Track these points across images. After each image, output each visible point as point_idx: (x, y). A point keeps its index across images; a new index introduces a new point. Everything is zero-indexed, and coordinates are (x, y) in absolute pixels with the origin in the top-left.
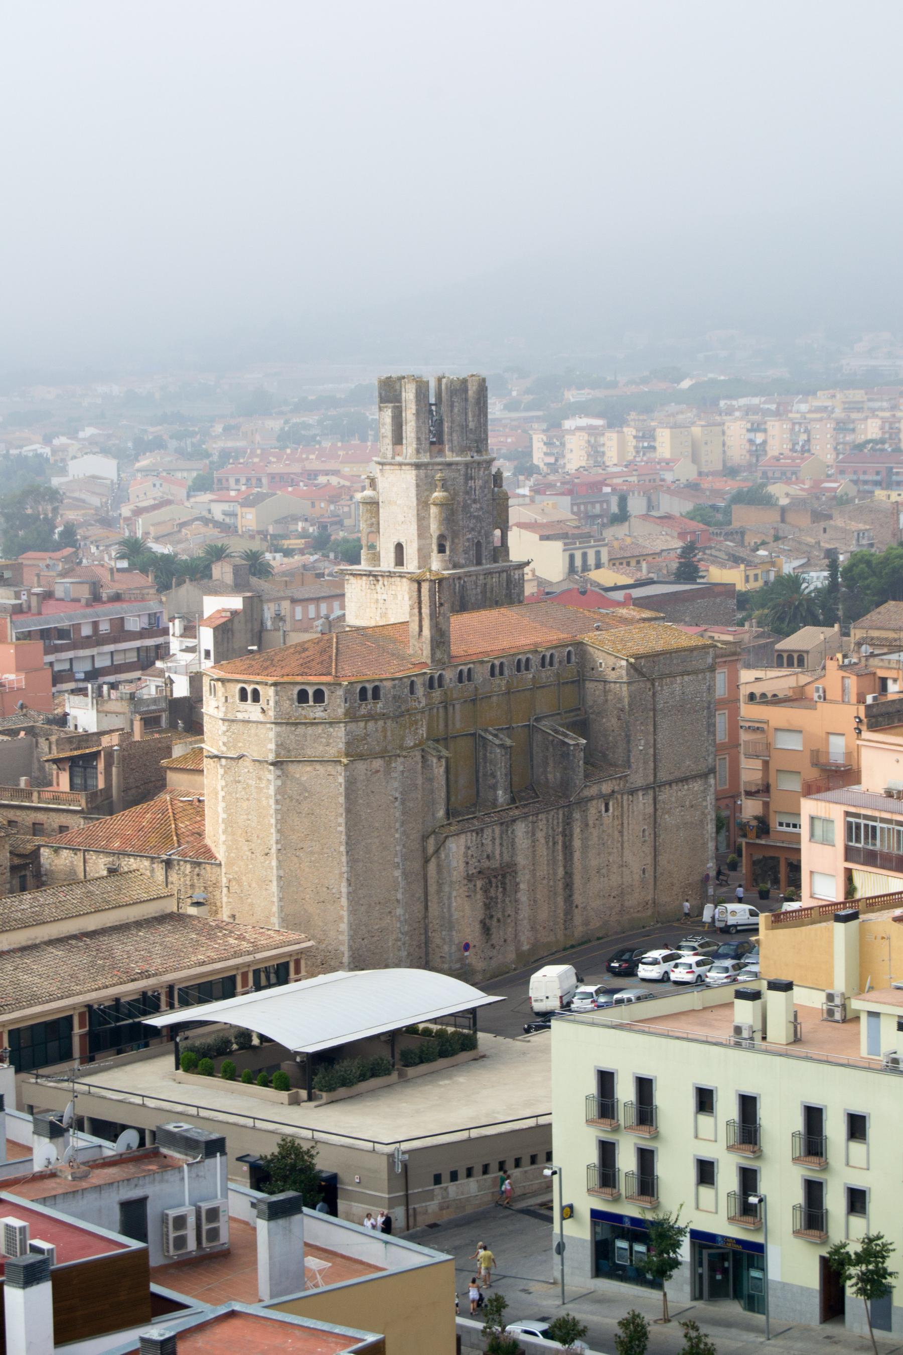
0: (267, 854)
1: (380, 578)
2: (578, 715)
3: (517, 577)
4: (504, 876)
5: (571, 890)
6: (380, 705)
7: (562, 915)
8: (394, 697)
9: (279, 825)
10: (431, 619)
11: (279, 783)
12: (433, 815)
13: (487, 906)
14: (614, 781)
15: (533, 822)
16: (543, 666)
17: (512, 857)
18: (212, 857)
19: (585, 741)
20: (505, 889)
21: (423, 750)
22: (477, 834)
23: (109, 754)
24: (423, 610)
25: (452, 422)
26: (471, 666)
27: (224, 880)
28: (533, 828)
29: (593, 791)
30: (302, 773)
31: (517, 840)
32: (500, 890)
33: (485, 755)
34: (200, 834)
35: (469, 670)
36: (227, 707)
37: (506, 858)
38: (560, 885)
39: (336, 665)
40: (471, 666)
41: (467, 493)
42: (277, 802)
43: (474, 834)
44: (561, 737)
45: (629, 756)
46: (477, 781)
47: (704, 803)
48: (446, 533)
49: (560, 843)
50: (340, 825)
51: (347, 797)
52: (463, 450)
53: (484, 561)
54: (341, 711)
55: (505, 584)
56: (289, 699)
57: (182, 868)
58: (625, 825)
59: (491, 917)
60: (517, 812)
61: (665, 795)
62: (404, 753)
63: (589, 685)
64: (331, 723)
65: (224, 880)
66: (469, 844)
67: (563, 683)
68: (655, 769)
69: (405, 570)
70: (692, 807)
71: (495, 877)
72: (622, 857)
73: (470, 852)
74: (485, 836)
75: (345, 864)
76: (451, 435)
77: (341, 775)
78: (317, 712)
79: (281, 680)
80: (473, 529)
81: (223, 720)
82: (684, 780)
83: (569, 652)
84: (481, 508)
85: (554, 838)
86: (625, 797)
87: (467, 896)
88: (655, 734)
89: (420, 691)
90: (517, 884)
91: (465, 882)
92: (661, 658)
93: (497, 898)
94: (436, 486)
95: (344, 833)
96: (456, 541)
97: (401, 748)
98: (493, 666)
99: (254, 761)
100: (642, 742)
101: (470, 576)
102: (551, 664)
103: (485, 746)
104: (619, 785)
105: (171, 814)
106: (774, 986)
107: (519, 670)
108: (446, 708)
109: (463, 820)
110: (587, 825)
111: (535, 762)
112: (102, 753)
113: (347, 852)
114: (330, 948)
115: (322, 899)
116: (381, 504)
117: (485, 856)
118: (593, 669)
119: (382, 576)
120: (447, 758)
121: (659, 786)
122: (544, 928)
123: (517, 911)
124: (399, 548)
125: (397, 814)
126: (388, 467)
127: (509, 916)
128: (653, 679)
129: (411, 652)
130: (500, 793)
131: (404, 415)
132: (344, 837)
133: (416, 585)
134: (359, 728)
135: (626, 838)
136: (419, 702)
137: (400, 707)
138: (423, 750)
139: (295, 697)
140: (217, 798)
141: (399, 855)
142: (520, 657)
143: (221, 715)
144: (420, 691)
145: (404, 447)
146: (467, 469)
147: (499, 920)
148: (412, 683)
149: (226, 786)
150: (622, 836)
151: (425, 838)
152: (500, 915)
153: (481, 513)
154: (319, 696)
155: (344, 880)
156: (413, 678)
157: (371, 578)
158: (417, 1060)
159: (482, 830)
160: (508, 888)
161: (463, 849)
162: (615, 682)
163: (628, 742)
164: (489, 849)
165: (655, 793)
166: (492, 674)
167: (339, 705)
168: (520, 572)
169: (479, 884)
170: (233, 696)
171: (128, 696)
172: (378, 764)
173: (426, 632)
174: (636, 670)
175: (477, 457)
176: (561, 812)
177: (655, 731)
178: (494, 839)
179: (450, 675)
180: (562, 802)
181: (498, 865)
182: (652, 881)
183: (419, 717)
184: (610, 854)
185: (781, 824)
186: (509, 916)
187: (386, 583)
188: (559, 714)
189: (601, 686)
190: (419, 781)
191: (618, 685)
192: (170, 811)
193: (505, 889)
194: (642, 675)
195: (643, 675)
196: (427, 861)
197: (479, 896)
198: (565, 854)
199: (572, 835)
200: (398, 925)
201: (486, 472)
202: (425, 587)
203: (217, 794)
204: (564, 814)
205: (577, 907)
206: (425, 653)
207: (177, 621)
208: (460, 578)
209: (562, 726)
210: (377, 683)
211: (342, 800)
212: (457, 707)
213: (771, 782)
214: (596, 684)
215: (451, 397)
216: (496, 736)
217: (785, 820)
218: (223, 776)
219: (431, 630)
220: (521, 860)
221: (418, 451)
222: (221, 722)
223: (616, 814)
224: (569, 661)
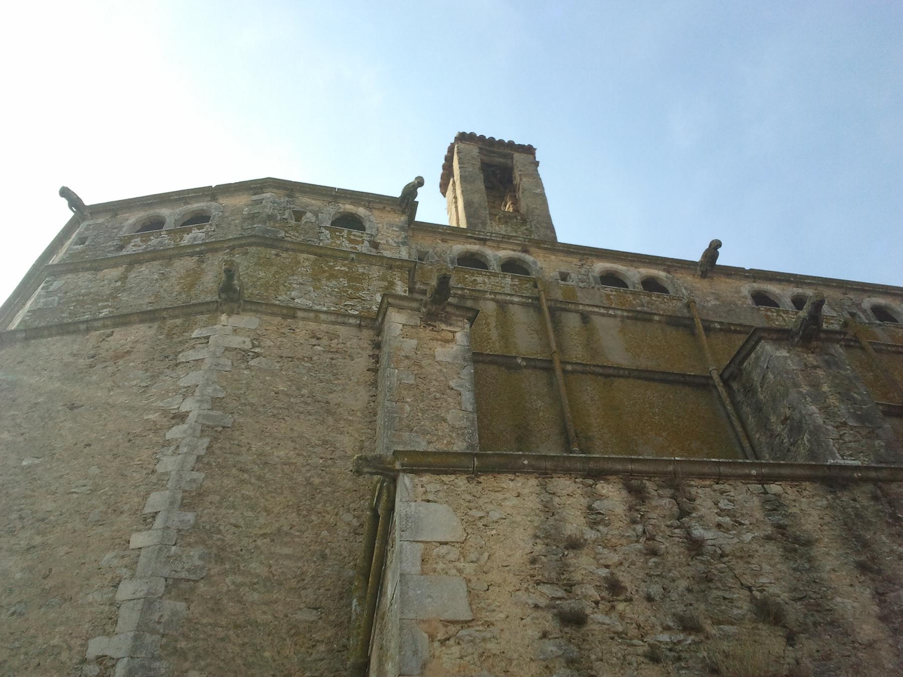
22: (638, 493)
66: (574, 523)
73: (583, 564)
161: (517, 545)
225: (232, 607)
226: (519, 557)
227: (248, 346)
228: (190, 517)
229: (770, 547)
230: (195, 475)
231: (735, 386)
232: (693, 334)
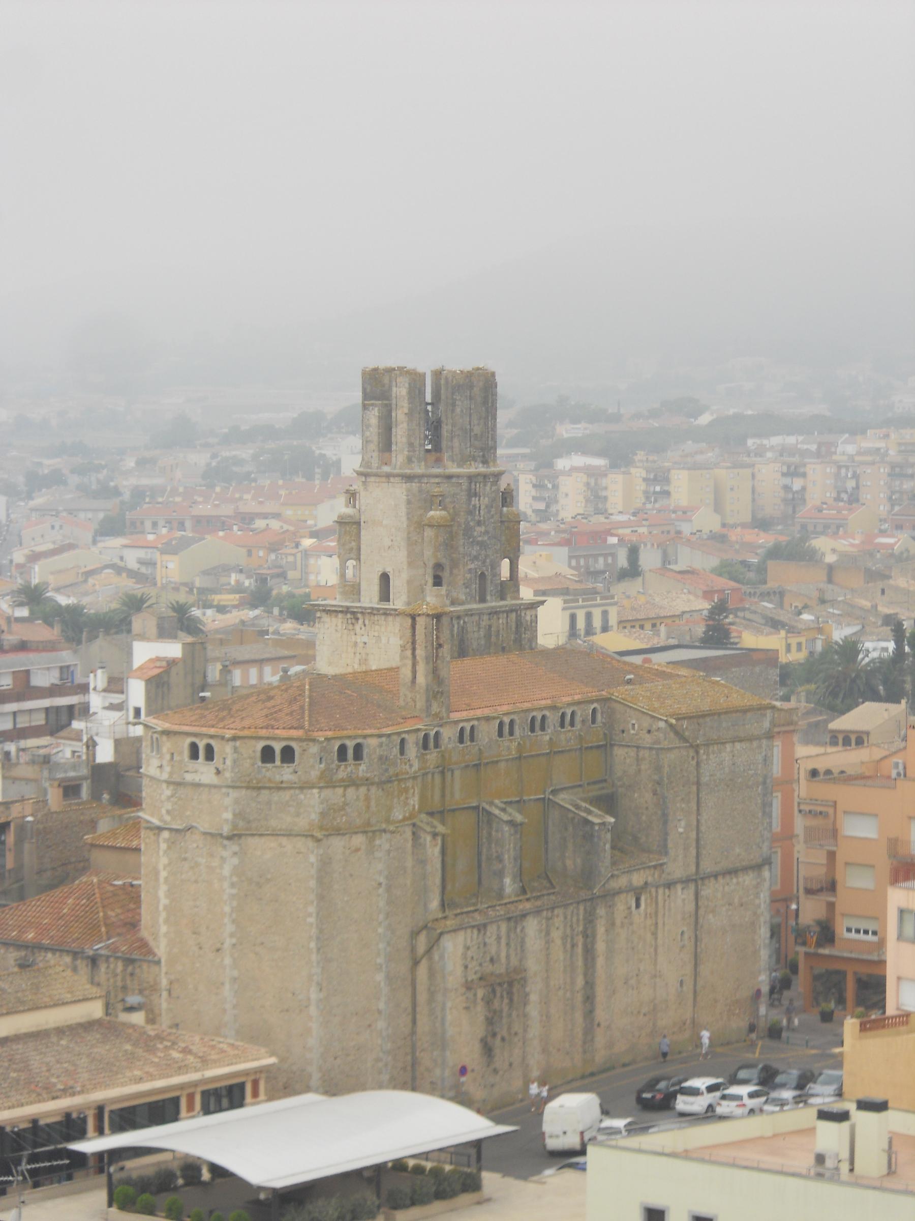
0: (218, 950)
1: (359, 615)
2: (603, 788)
3: (528, 618)
4: (511, 984)
6: (362, 769)
8: (380, 758)
9: (234, 916)
10: (427, 663)
11: (235, 861)
12: (425, 905)
13: (490, 1022)
14: (647, 872)
15: (548, 919)
16: (562, 725)
17: (521, 960)
18: (150, 952)
19: (612, 820)
20: (511, 1000)
21: (414, 825)
22: (479, 930)
23: (22, 827)
24: (418, 652)
25: (453, 425)
26: (476, 723)
27: (164, 982)
29: (622, 881)
30: (262, 850)
31: (527, 940)
32: (506, 1001)
33: (490, 834)
34: (133, 925)
35: (472, 728)
36: (172, 766)
37: (514, 961)
38: (579, 998)
39: (310, 716)
40: (476, 723)
41: (470, 513)
42: (233, 885)
43: (475, 931)
44: (583, 814)
45: (666, 840)
46: (479, 866)
47: (757, 901)
48: (443, 561)
50: (310, 915)
51: (320, 880)
52: (463, 460)
53: (488, 598)
54: (314, 774)
55: (514, 629)
56: (250, 758)
57: (112, 966)
59: (494, 1035)
60: (528, 906)
61: (709, 890)
62: (392, 828)
63: (619, 752)
64: (301, 788)
65: (164, 982)
67: (587, 748)
69: (392, 607)
71: (500, 984)
72: (655, 964)
73: (469, 953)
74: (488, 933)
75: (315, 964)
76: (452, 441)
77: (312, 852)
78: (286, 773)
79: (241, 734)
80: (476, 558)
81: (168, 783)
82: (732, 872)
83: (594, 710)
84: (486, 532)
85: (572, 938)
86: (661, 891)
87: (467, 1008)
88: (698, 813)
89: (412, 751)
90: (527, 995)
91: (464, 990)
92: (708, 719)
93: (501, 1011)
94: (432, 503)
95: (314, 926)
96: (455, 571)
97: (388, 821)
98: (501, 724)
99: (205, 834)
100: (683, 823)
101: (472, 615)
102: (572, 724)
103: (489, 823)
105: (98, 900)
106: (865, 1105)
107: (532, 730)
108: (442, 773)
109: (462, 913)
110: (613, 924)
112: (12, 825)
113: (318, 950)
116: (362, 523)
117: (488, 959)
118: (623, 732)
119: (362, 613)
120: (443, 836)
121: (702, 879)
122: (559, 1050)
123: (526, 1029)
124: (385, 578)
125: (382, 904)
126: (372, 479)
127: (516, 1034)
128: (698, 746)
129: (402, 703)
130: (507, 881)
131: (394, 414)
132: (314, 931)
133: (410, 621)
134: (335, 795)
135: (660, 942)
136: (411, 766)
137: (387, 770)
138: (414, 825)
139: (259, 754)
140: (157, 879)
142: (534, 713)
143: (165, 776)
144: (412, 751)
145: (394, 455)
146: (470, 483)
147: (503, 1039)
148: (403, 741)
149: (170, 864)
150: (656, 939)
151: (414, 934)
152: (504, 1033)
153: (486, 538)
154: (288, 755)
156: (403, 736)
157: (349, 616)
158: (408, 1202)
159: (485, 926)
160: (515, 998)
161: (460, 950)
162: (650, 749)
163: (665, 823)
164: (493, 950)
165: (697, 886)
166: (500, 734)
168: (533, 612)
169: (480, 993)
170: (181, 753)
171: (41, 759)
172: (359, 840)
173: (421, 679)
174: (677, 733)
175: (482, 469)
176: (582, 908)
177: (698, 809)
178: (499, 938)
179: (448, 734)
180: (583, 894)
181: (503, 970)
182: (691, 996)
183: (410, 784)
185: (849, 930)
187: (367, 622)
188: (580, 786)
189: (632, 753)
190: (409, 863)
191: (654, 752)
192: (97, 895)
193: (511, 1000)
194: (685, 740)
195: (685, 740)
196: (416, 963)
197: (480, 1008)
198: (586, 959)
199: (594, 937)
200: (379, 1042)
201: (494, 488)
202: (421, 622)
203: (157, 873)
204: (585, 909)
205: (599, 1025)
206: (419, 705)
207: (99, 672)
208: (459, 618)
209: (584, 800)
210: (359, 741)
211: (313, 883)
212: (457, 773)
213: (838, 877)
214: (626, 750)
215: (453, 394)
216: (504, 810)
217: (854, 924)
218: (165, 852)
219: (426, 676)
220: (533, 965)
221: (409, 460)
222: (164, 786)
223: (649, 911)
224: (594, 721)
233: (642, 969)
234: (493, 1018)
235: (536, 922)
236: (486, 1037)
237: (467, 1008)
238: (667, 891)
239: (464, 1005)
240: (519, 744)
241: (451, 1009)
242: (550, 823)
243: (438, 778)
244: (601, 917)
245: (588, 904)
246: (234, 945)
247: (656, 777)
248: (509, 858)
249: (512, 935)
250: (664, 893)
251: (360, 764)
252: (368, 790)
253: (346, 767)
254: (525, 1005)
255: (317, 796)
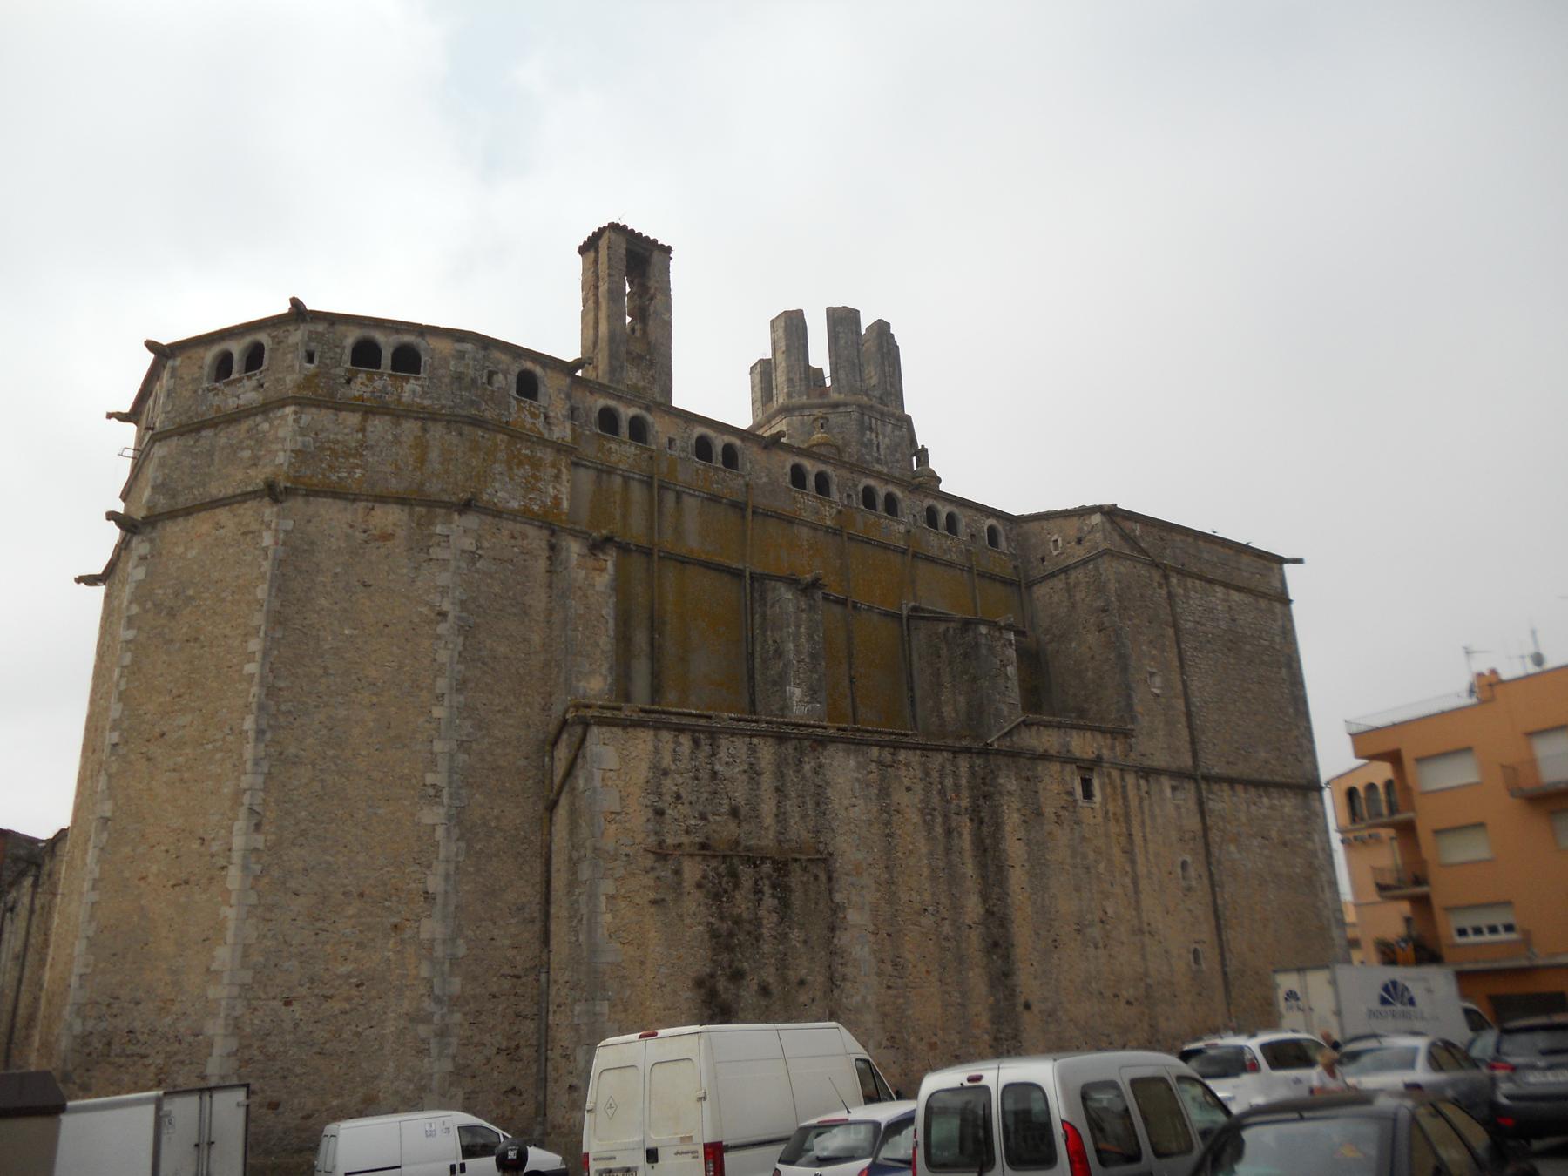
4: (782, 867)
5: (1006, 957)
6: (411, 388)
7: (984, 1020)
13: (721, 941)
14: (1099, 737)
20: (784, 904)
22: (696, 742)
28: (883, 778)
32: (769, 902)
33: (764, 616)
37: (798, 830)
38: (974, 940)
43: (685, 740)
45: (1129, 697)
46: (752, 678)
49: (967, 836)
50: (250, 658)
58: (1138, 838)
59: (737, 976)
66: (667, 761)
68: (1193, 742)
70: (1285, 844)
71: (752, 861)
72: (1138, 908)
73: (668, 783)
74: (723, 754)
75: (249, 766)
77: (268, 527)
78: (247, 393)
85: (946, 817)
87: (654, 902)
91: (649, 861)
93: (758, 923)
95: (256, 680)
100: (1158, 680)
104: (1112, 748)
110: (1039, 814)
111: (918, 693)
113: (260, 732)
114: (182, 1026)
115: (184, 876)
118: (1043, 560)
122: (933, 1046)
125: (443, 656)
130: (796, 692)
135: (1142, 869)
141: (443, 764)
147: (765, 990)
150: (1133, 862)
152: (770, 975)
155: (243, 812)
159: (713, 734)
160: (797, 900)
161: (642, 772)
163: (1125, 669)
164: (740, 792)
167: (291, 368)
169: (692, 870)
172: (390, 517)
178: (754, 773)
181: (768, 840)
182: (1218, 981)
184: (1106, 896)
185: (1462, 932)
186: (802, 983)
193: (784, 904)
196: (552, 806)
197: (693, 904)
198: (982, 866)
199: (998, 826)
200: (425, 971)
204: (971, 767)
205: (1027, 1006)
210: (408, 338)
211: (262, 591)
212: (690, 503)
214: (1050, 583)
217: (1467, 921)
220: (848, 849)
221: (789, 395)
223: (1111, 807)
225: (489, 758)
226: (642, 780)
227: (473, 548)
228: (461, 698)
229: (745, 777)
230: (462, 667)
231: (756, 585)
232: (743, 517)
233: (1110, 911)
234: (731, 935)
235: (852, 763)
236: (712, 976)
237: (654, 902)
238: (1142, 782)
239: (652, 896)
240: (840, 512)
241: (611, 898)
242: (915, 658)
243: (637, 493)
244: (1010, 794)
245: (979, 761)
246: (115, 745)
247: (1100, 603)
248: (798, 652)
249: (790, 773)
250: (1138, 787)
251: (407, 380)
252: (425, 430)
253: (371, 380)
254: (832, 929)
255: (291, 418)
